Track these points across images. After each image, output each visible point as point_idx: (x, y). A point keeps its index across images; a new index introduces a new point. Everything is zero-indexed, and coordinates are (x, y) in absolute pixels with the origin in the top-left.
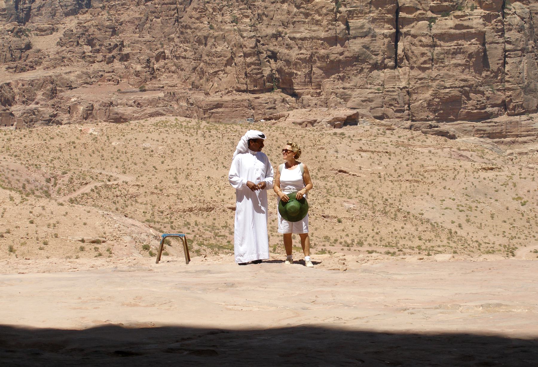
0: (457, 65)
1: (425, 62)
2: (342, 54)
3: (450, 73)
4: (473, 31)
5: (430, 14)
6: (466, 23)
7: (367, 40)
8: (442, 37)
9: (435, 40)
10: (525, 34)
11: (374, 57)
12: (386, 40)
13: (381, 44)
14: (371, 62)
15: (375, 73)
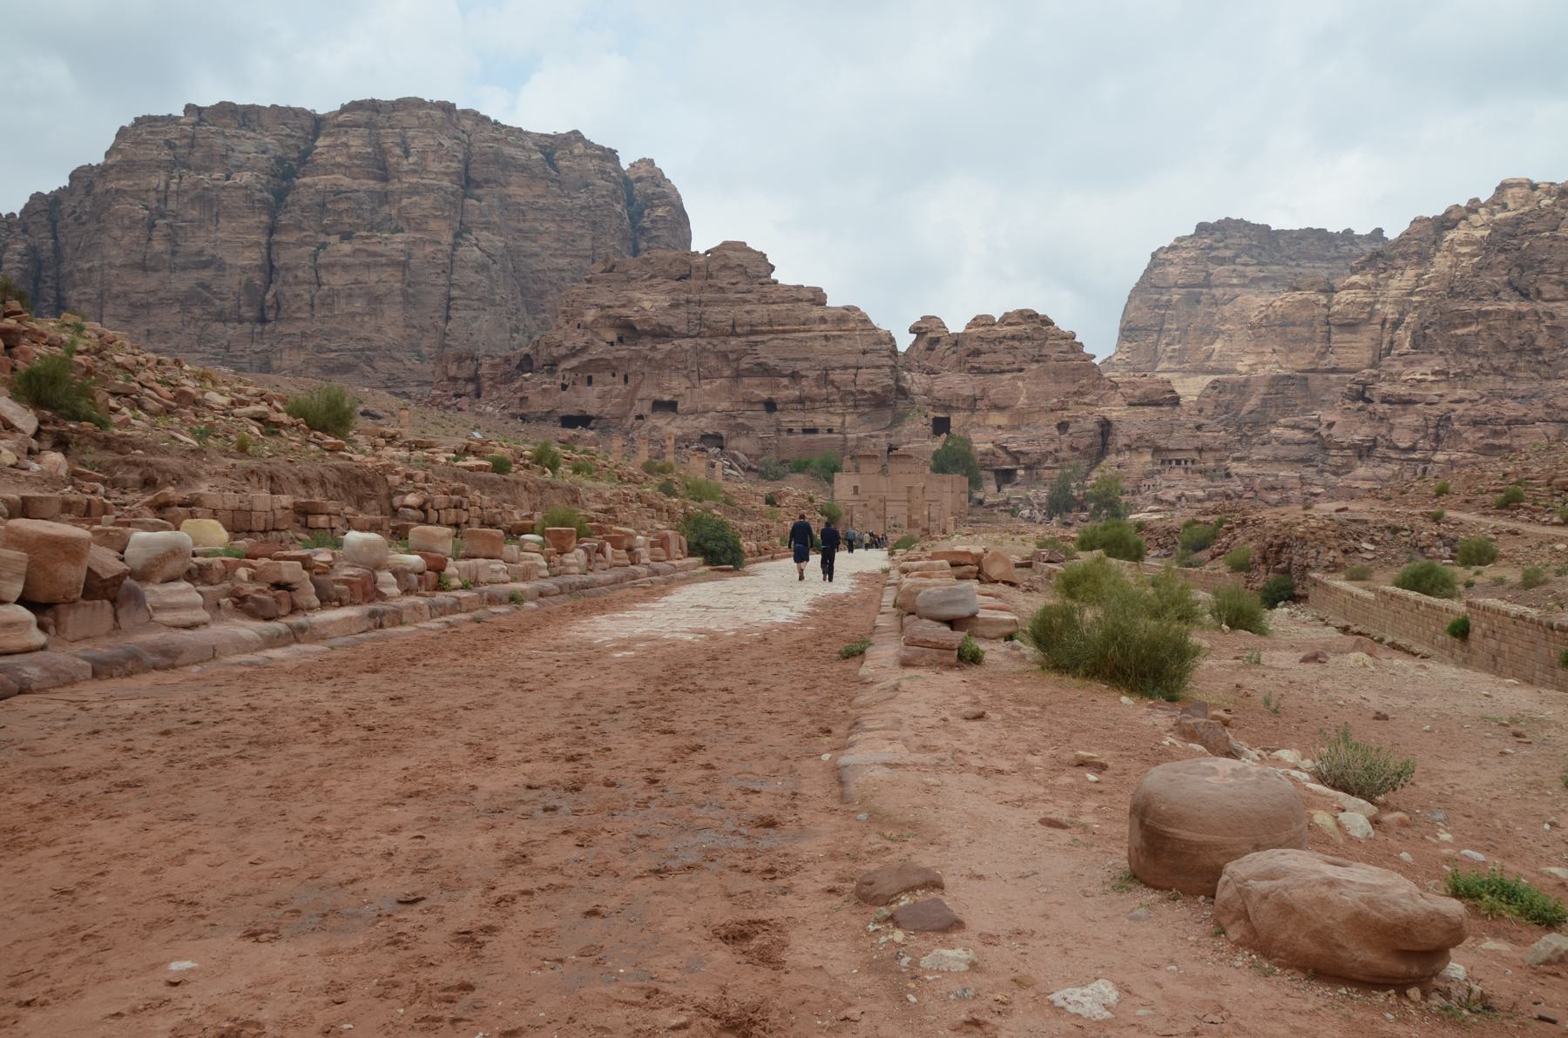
0: (353, 315)
1: (299, 309)
2: (154, 292)
3: (343, 328)
4: (383, 260)
5: (322, 238)
6: (371, 248)
7: (207, 274)
8: (330, 267)
9: (322, 273)
10: (490, 278)
11: (217, 302)
12: (244, 278)
13: (231, 283)
14: (211, 310)
15: (217, 327)
